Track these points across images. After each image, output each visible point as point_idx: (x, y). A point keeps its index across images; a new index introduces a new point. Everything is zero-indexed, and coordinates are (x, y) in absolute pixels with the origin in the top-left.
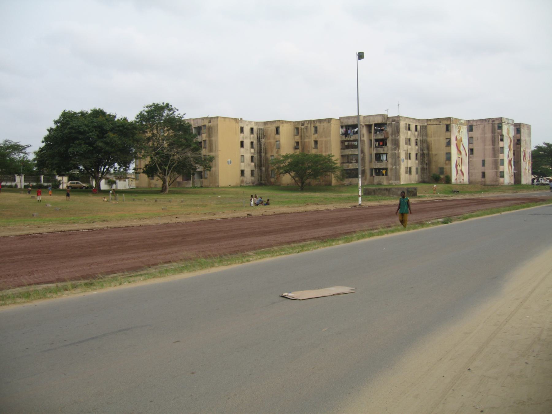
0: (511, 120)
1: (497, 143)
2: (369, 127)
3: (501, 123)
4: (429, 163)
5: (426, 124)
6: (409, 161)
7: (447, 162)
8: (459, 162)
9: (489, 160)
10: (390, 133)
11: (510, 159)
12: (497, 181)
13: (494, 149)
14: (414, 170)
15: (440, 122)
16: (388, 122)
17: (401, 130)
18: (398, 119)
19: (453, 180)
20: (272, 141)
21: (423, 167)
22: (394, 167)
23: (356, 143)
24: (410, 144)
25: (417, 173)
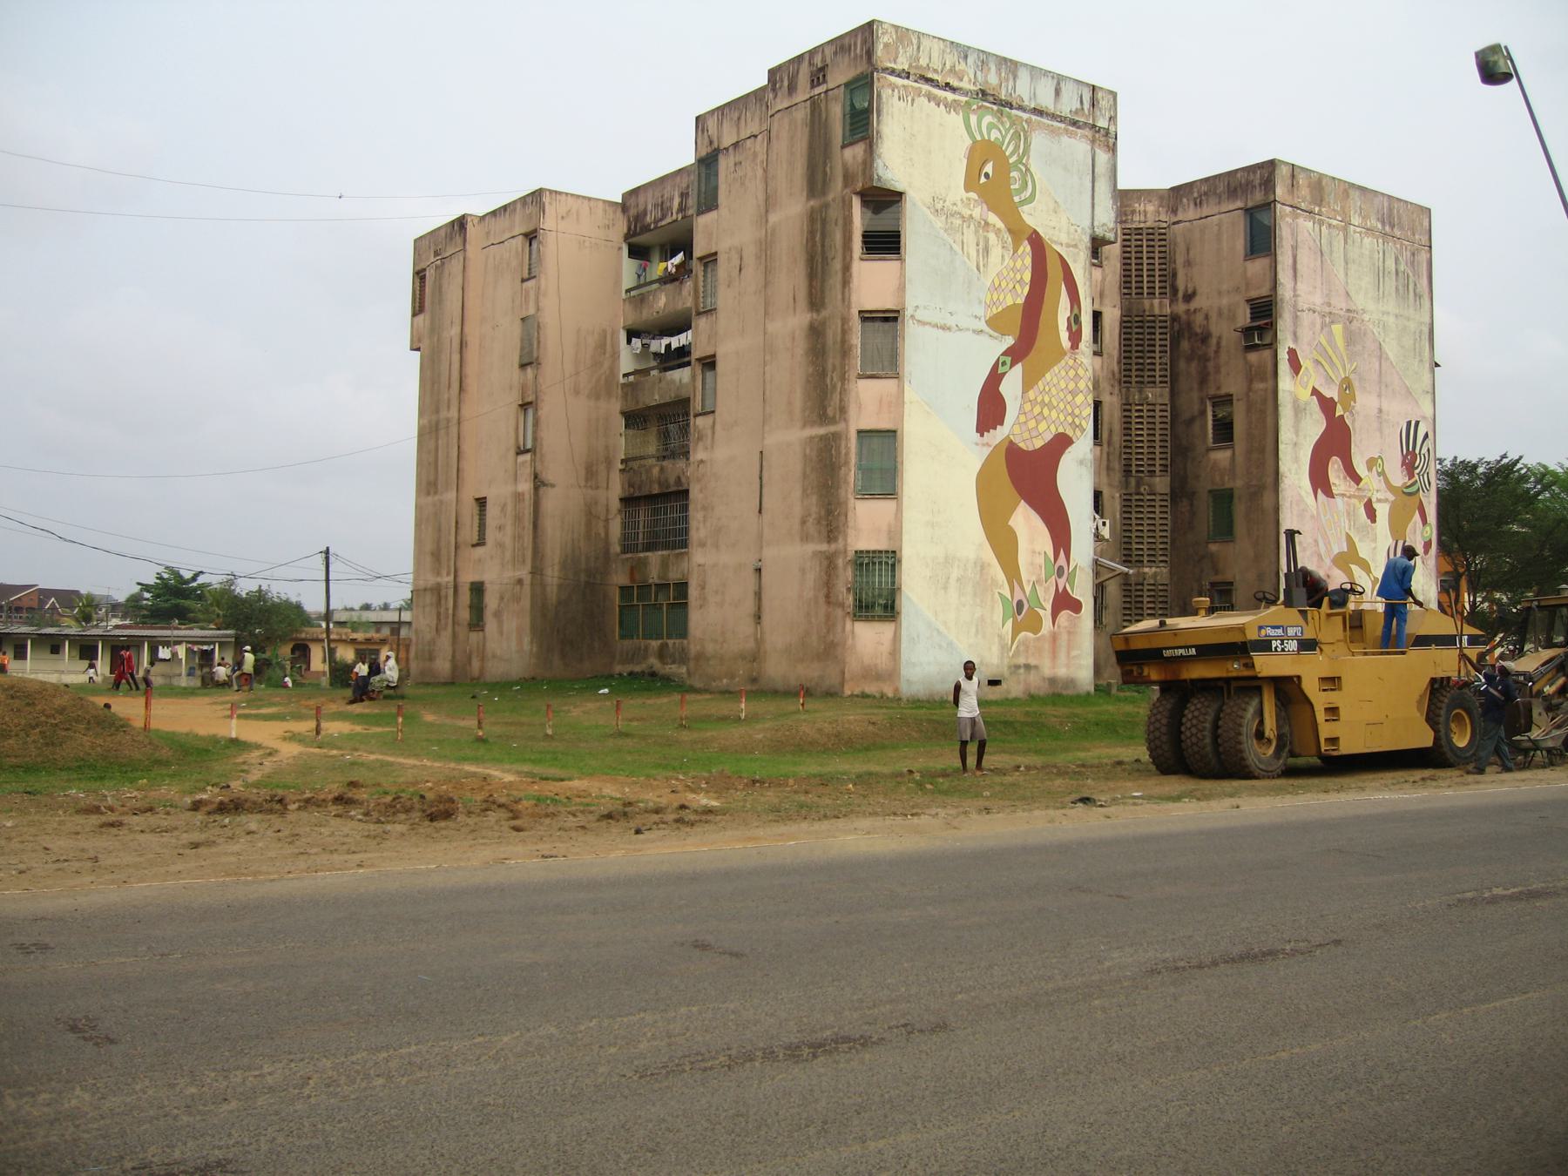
12: (830, 649)
13: (816, 332)
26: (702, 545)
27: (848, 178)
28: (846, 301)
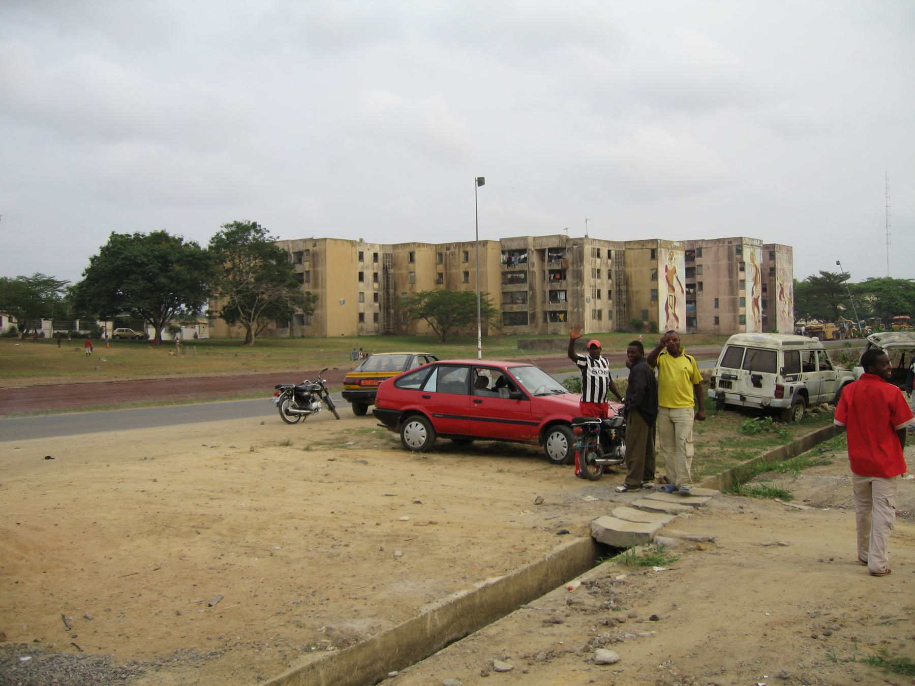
0: (758, 240)
1: (735, 275)
2: (541, 252)
3: (741, 246)
4: (628, 304)
5: (624, 249)
6: (598, 301)
7: (652, 302)
8: (671, 302)
9: (724, 298)
10: (570, 261)
11: (756, 297)
13: (731, 283)
14: (605, 314)
15: (643, 246)
16: (568, 246)
17: (585, 257)
18: (582, 242)
19: (662, 328)
20: (404, 272)
21: (620, 310)
22: (575, 310)
23: (522, 276)
24: (599, 277)
25: (610, 317)
26: (700, 312)
27: (737, 260)
28: (737, 278)
